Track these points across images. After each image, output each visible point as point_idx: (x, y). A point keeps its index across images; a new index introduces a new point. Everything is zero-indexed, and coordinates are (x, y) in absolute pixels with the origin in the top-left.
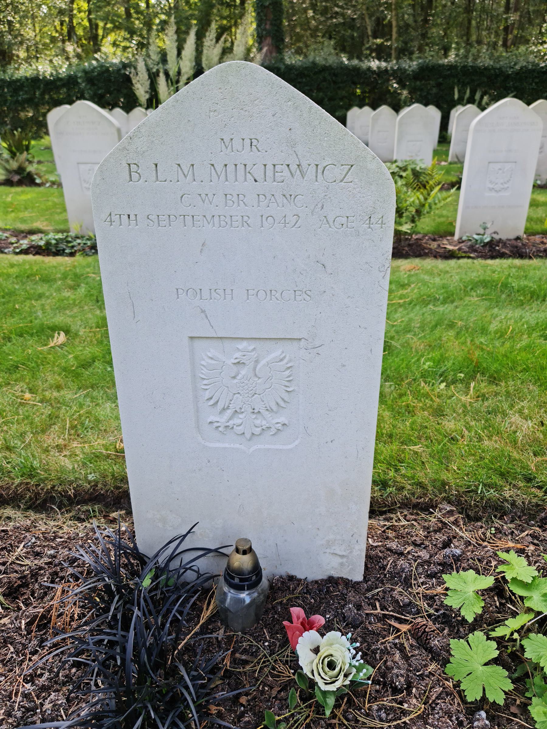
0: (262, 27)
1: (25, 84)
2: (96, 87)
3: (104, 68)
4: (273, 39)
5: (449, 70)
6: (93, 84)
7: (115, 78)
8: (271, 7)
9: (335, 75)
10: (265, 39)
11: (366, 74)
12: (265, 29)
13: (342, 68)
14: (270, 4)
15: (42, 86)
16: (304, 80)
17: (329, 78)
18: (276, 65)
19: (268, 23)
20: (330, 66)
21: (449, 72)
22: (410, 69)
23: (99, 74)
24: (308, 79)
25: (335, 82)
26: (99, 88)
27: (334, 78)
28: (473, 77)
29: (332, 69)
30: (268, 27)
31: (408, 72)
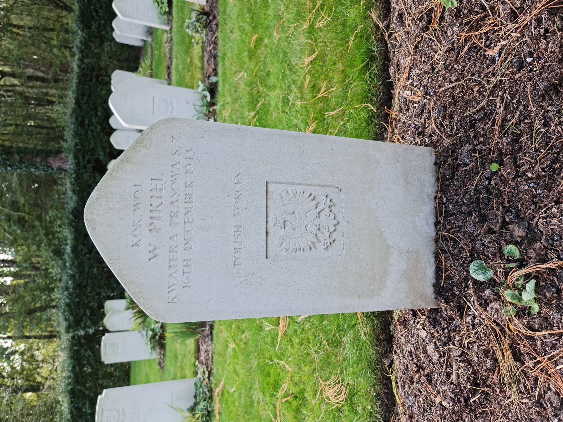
0: (38, 165)
1: (76, 406)
2: (84, 318)
3: (67, 309)
4: (49, 156)
6: (81, 320)
7: (76, 297)
8: (21, 155)
9: (83, 95)
10: (49, 163)
11: (84, 69)
12: (41, 162)
14: (19, 155)
15: (78, 387)
16: (86, 122)
17: (85, 100)
19: (35, 159)
23: (72, 314)
25: (90, 96)
26: (85, 315)
27: (86, 96)
30: (38, 160)
31: (84, 34)
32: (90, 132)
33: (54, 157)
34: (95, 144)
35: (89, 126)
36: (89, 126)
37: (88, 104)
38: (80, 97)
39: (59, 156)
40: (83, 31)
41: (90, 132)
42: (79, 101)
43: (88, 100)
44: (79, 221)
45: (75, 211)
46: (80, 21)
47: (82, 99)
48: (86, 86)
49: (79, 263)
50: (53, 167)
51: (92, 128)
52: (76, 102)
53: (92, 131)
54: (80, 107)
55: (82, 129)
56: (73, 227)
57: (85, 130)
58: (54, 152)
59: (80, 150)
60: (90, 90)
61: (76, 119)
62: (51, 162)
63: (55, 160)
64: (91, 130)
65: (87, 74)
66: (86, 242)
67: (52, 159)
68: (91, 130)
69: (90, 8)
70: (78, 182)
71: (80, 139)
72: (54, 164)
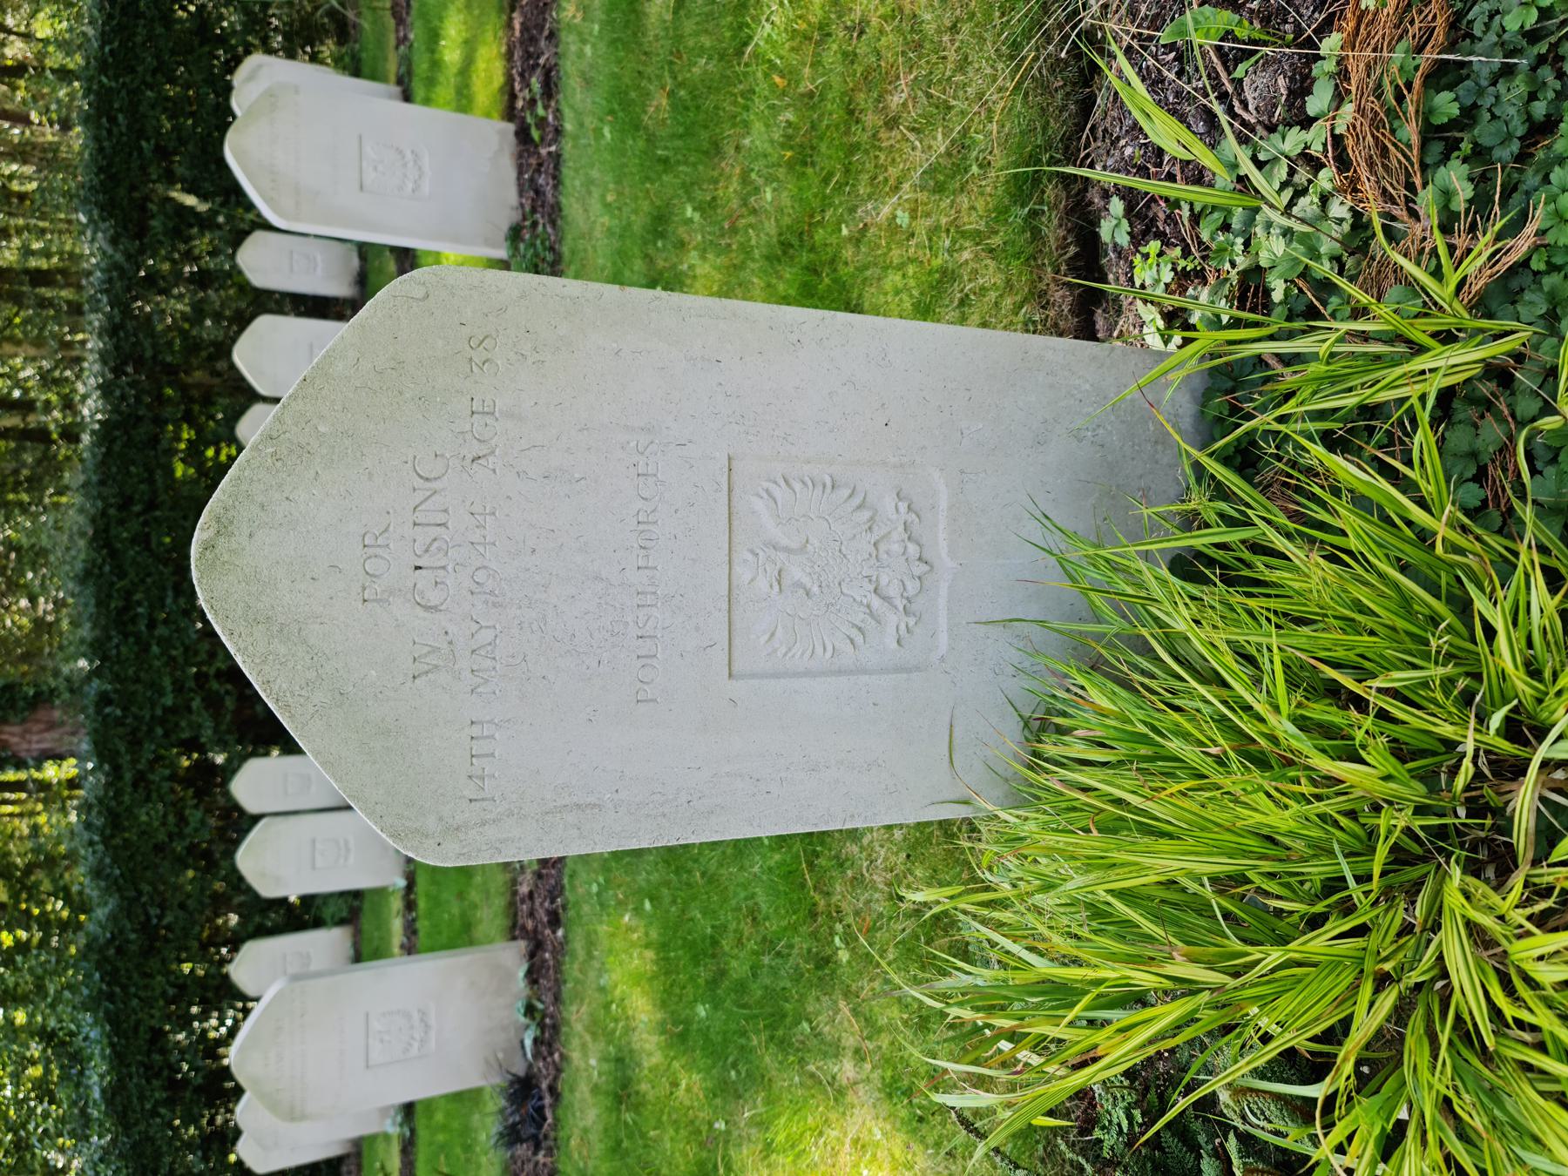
5: (113, 120)
9: (126, 503)
13: (102, 483)
17: (135, 525)
18: (91, 711)
20: (93, 521)
21: (120, 117)
22: (110, 251)
24: (138, 597)
25: (151, 505)
27: (137, 508)
28: (139, 39)
29: (104, 513)
31: (119, 257)
32: (155, 649)
33: (24, 721)
34: (179, 688)
35: (152, 625)
36: (152, 625)
37: (147, 535)
38: (112, 511)
39: (42, 714)
40: (114, 241)
41: (155, 649)
42: (106, 530)
43: (145, 524)
44: (124, 988)
45: (112, 952)
46: (102, 209)
47: (121, 522)
48: (133, 469)
49: (133, 1147)
50: (23, 754)
51: (162, 631)
52: (94, 539)
53: (165, 642)
54: (113, 554)
55: (126, 636)
56: (107, 1012)
57: (138, 641)
58: (21, 704)
59: (119, 722)
60: (151, 481)
61: (98, 604)
62: (14, 740)
63: (27, 731)
64: (161, 641)
65: (139, 419)
66: (157, 1057)
67: (16, 729)
68: (161, 641)
69: (140, 149)
70: (117, 841)
71: (117, 678)
72: (25, 746)
